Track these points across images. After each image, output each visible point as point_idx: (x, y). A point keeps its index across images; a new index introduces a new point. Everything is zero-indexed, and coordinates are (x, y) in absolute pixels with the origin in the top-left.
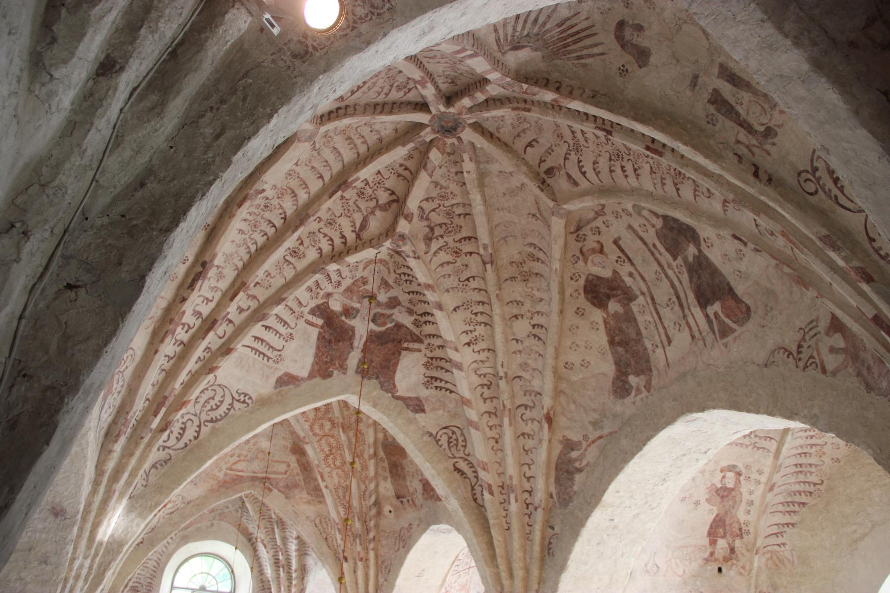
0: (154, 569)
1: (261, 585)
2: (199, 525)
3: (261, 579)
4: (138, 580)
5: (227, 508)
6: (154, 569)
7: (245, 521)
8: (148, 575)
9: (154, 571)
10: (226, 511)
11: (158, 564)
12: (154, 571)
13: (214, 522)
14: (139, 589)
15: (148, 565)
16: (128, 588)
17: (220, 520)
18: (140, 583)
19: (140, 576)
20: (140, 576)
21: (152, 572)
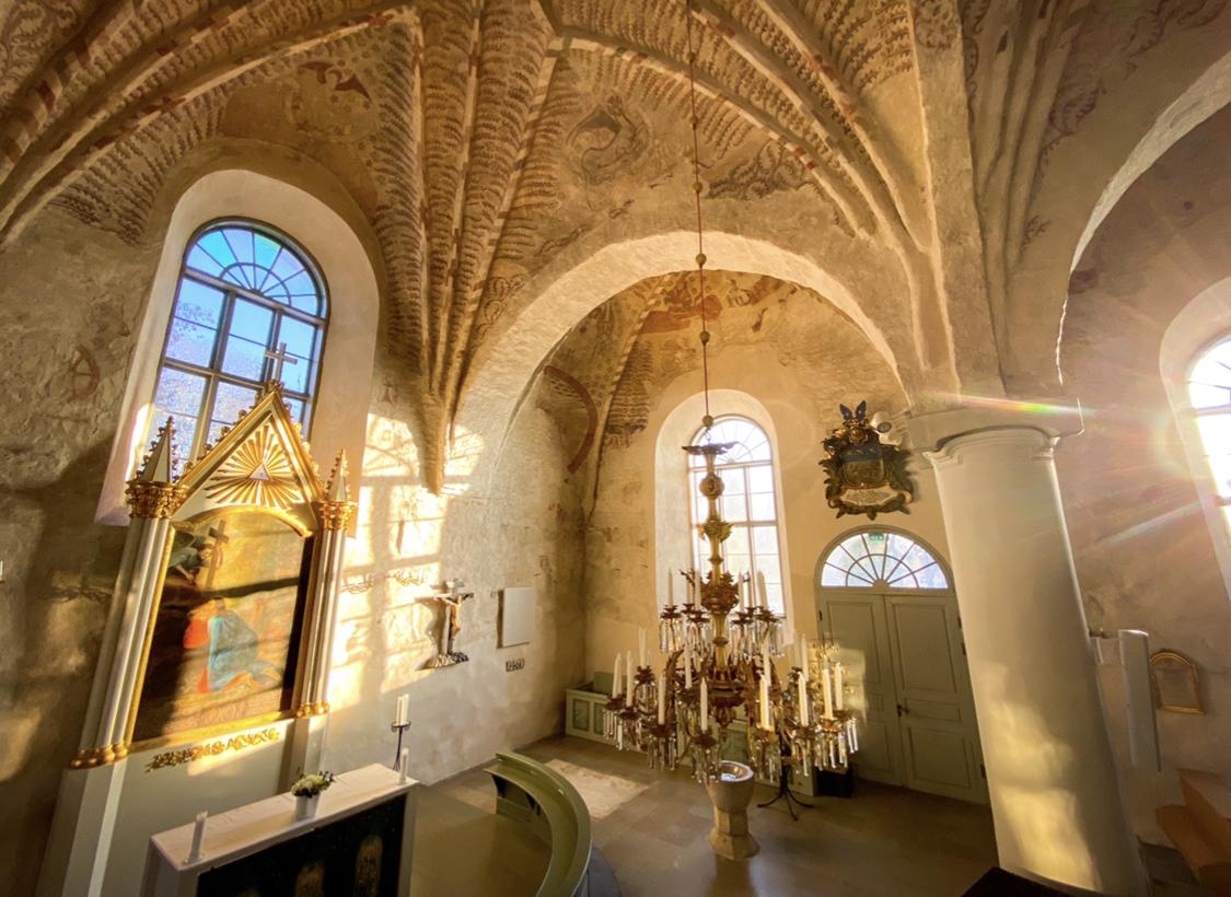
0: (145, 183)
1: (394, 308)
2: (266, 143)
3: (395, 299)
4: (93, 189)
5: (340, 132)
6: (145, 183)
7: (374, 174)
8: (126, 191)
9: (145, 188)
10: (333, 139)
11: (156, 176)
12: (145, 188)
13: (303, 156)
14: (97, 213)
15: (126, 161)
16: (51, 194)
17: (313, 157)
18: (99, 201)
19: (101, 182)
20: (101, 182)
21: (140, 189)
